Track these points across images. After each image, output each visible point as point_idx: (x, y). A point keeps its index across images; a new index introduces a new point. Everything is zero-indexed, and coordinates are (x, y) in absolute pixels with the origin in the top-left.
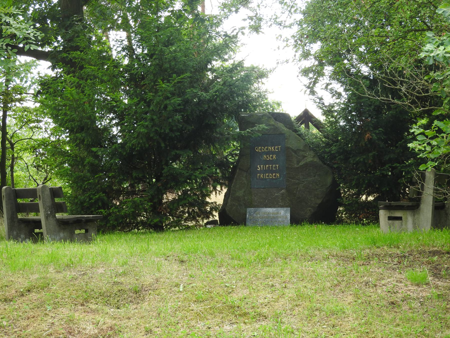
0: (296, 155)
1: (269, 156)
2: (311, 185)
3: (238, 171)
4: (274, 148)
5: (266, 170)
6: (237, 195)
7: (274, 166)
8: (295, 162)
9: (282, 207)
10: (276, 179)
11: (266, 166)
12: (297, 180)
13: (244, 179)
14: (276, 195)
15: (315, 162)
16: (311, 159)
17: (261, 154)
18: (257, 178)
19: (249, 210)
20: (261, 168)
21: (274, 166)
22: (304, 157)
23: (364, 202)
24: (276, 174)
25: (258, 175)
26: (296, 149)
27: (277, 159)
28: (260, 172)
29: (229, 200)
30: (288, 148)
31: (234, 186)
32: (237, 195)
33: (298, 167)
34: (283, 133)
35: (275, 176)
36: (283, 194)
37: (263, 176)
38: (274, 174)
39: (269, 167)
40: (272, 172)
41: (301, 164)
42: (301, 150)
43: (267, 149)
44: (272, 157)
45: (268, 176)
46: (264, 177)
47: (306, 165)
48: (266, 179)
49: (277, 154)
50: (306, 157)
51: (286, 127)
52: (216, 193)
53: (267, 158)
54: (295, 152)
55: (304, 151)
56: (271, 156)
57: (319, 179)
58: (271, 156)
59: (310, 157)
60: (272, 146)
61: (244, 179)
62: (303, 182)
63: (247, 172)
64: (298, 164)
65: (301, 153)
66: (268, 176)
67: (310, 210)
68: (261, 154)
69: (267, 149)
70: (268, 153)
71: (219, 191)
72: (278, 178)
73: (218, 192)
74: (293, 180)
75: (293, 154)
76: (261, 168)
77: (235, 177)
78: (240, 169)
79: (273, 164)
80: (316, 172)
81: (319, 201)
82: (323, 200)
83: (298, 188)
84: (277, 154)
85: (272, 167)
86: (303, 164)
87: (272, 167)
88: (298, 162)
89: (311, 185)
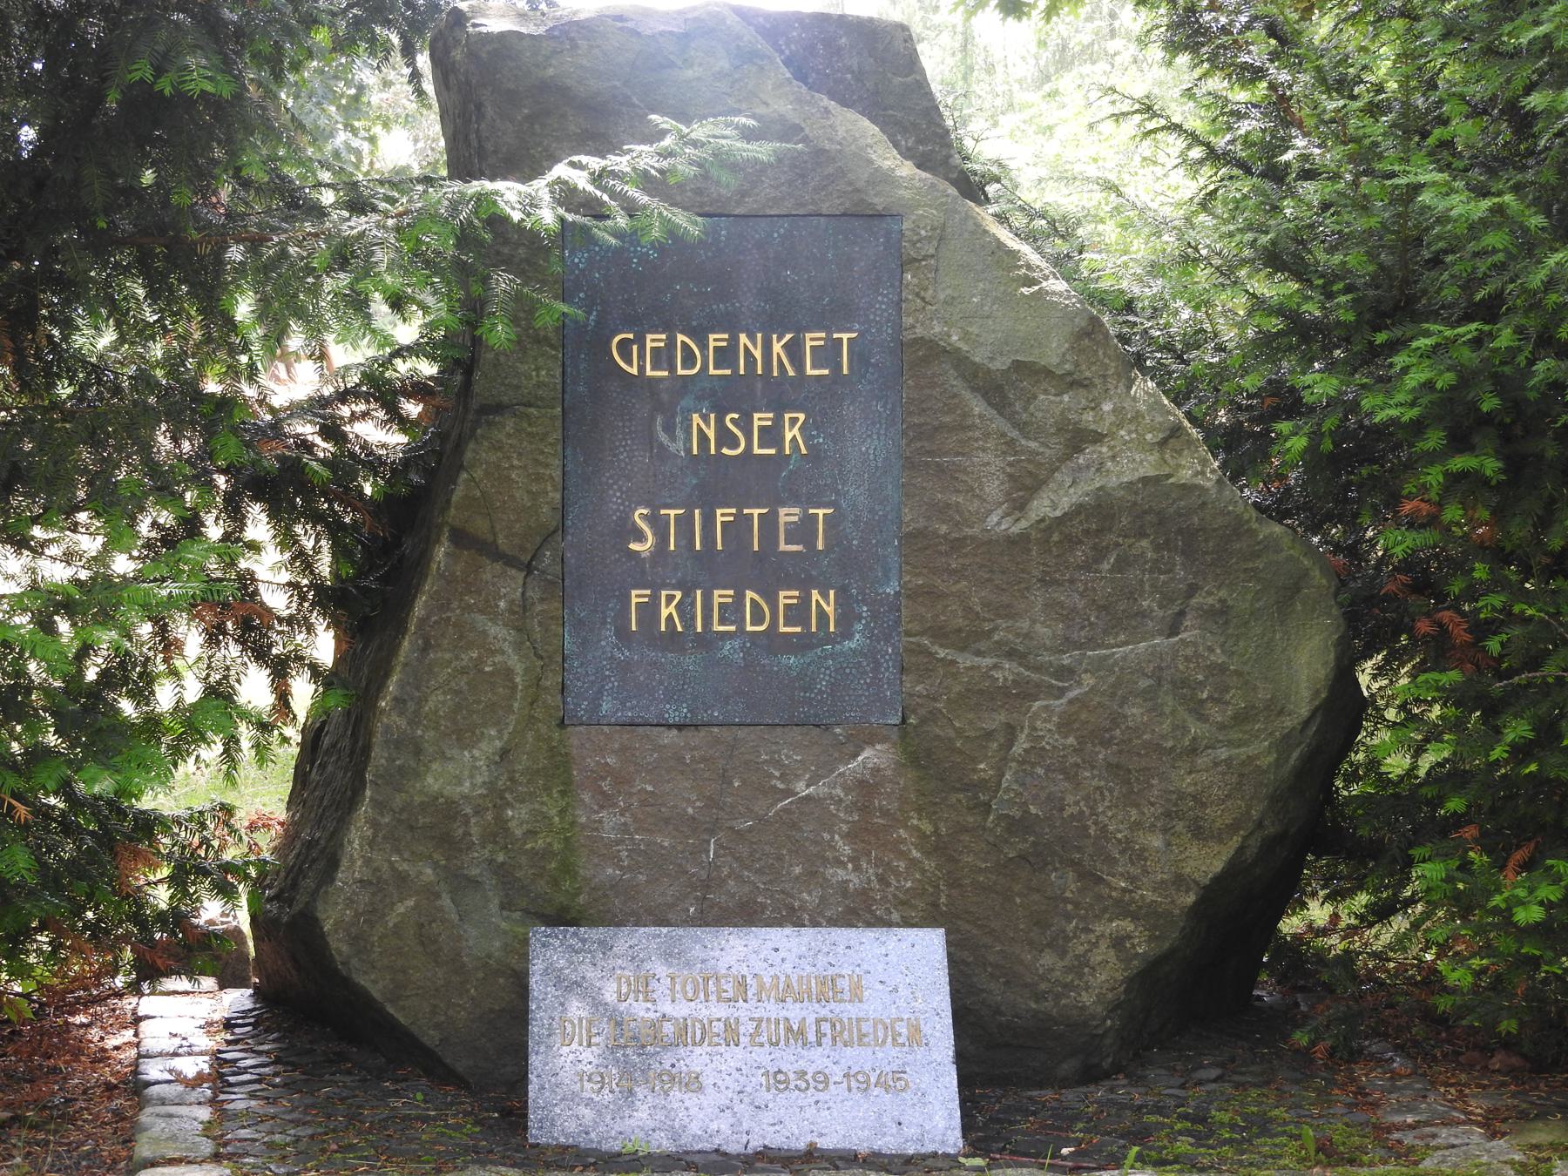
0: (1000, 424)
1: (746, 426)
2: (1135, 712)
3: (441, 552)
4: (794, 350)
5: (715, 555)
6: (432, 783)
7: (788, 515)
8: (993, 488)
9: (859, 912)
10: (802, 644)
11: (709, 521)
12: (1011, 654)
13: (498, 632)
14: (802, 789)
15: (1187, 489)
16: (1146, 465)
17: (667, 401)
18: (623, 632)
19: (551, 957)
20: (662, 537)
21: (788, 515)
22: (1078, 439)
23: (1361, 726)
24: (805, 600)
25: (637, 596)
26: (1000, 364)
27: (815, 454)
28: (653, 573)
29: (356, 838)
30: (933, 351)
31: (398, 701)
32: (432, 783)
33: (1024, 537)
34: (879, 202)
35: (798, 613)
36: (866, 788)
37: (685, 609)
38: (787, 597)
39: (738, 528)
40: (767, 571)
41: (1044, 506)
42: (1048, 373)
43: (726, 356)
44: (772, 435)
45: (732, 612)
46: (688, 619)
47: (1099, 515)
48: (708, 641)
49: (819, 402)
50: (1098, 438)
51: (907, 154)
52: (231, 744)
53: (725, 438)
54: (994, 389)
55: (1074, 383)
56: (761, 419)
57: (1218, 657)
58: (761, 419)
59: (1137, 443)
60: (771, 324)
61: (498, 632)
62: (1066, 673)
63: (528, 568)
64: (1020, 507)
65: (1050, 404)
66: (732, 612)
67: (1118, 942)
68: (667, 401)
69: (726, 356)
70: (731, 396)
71: (264, 727)
72: (829, 638)
73: (246, 734)
74: (965, 660)
75: (978, 406)
76: (662, 537)
77: (419, 608)
78: (461, 538)
79: (776, 502)
80: (1192, 590)
81: (1207, 862)
82: (1241, 850)
83: (1011, 731)
84: (819, 402)
85: (769, 522)
86: (1065, 504)
87: (769, 522)
88: (1024, 486)
89: (1135, 712)
